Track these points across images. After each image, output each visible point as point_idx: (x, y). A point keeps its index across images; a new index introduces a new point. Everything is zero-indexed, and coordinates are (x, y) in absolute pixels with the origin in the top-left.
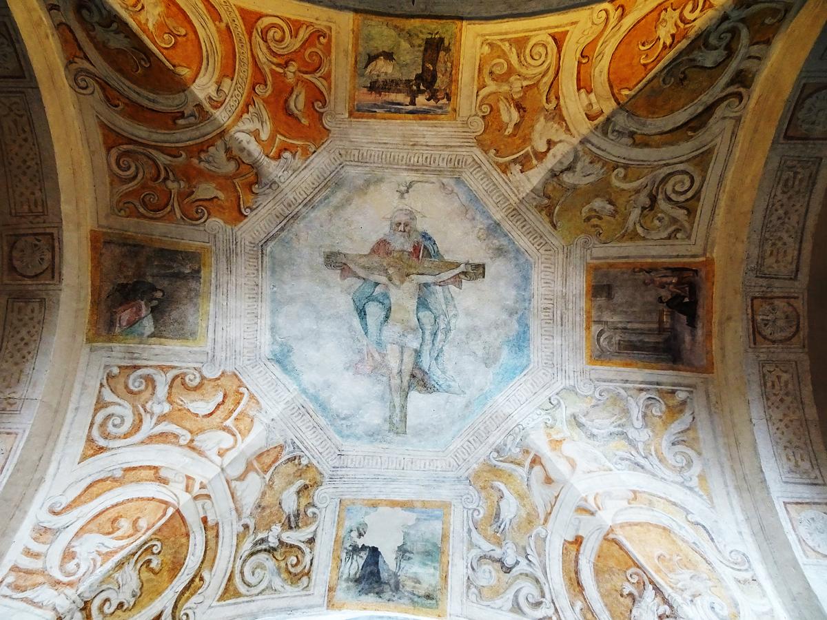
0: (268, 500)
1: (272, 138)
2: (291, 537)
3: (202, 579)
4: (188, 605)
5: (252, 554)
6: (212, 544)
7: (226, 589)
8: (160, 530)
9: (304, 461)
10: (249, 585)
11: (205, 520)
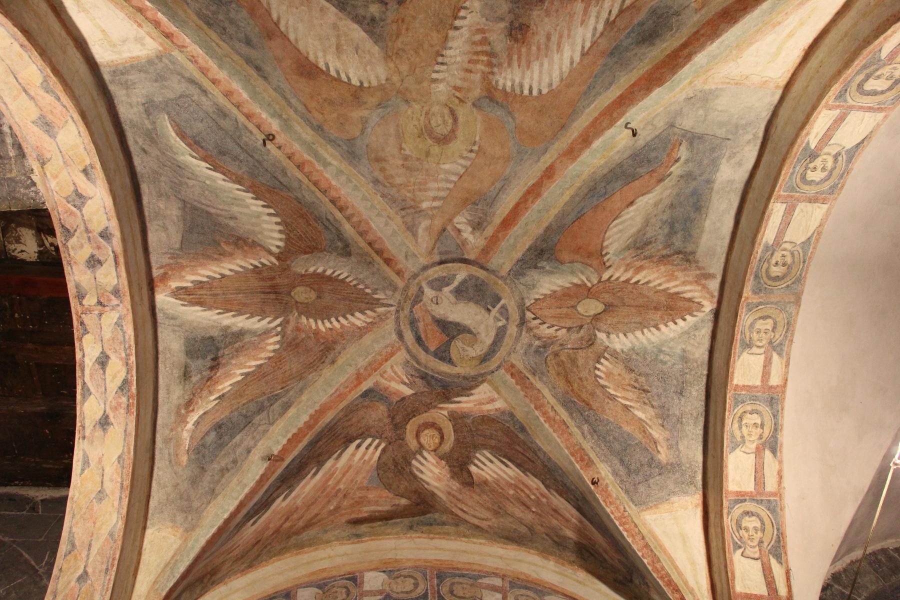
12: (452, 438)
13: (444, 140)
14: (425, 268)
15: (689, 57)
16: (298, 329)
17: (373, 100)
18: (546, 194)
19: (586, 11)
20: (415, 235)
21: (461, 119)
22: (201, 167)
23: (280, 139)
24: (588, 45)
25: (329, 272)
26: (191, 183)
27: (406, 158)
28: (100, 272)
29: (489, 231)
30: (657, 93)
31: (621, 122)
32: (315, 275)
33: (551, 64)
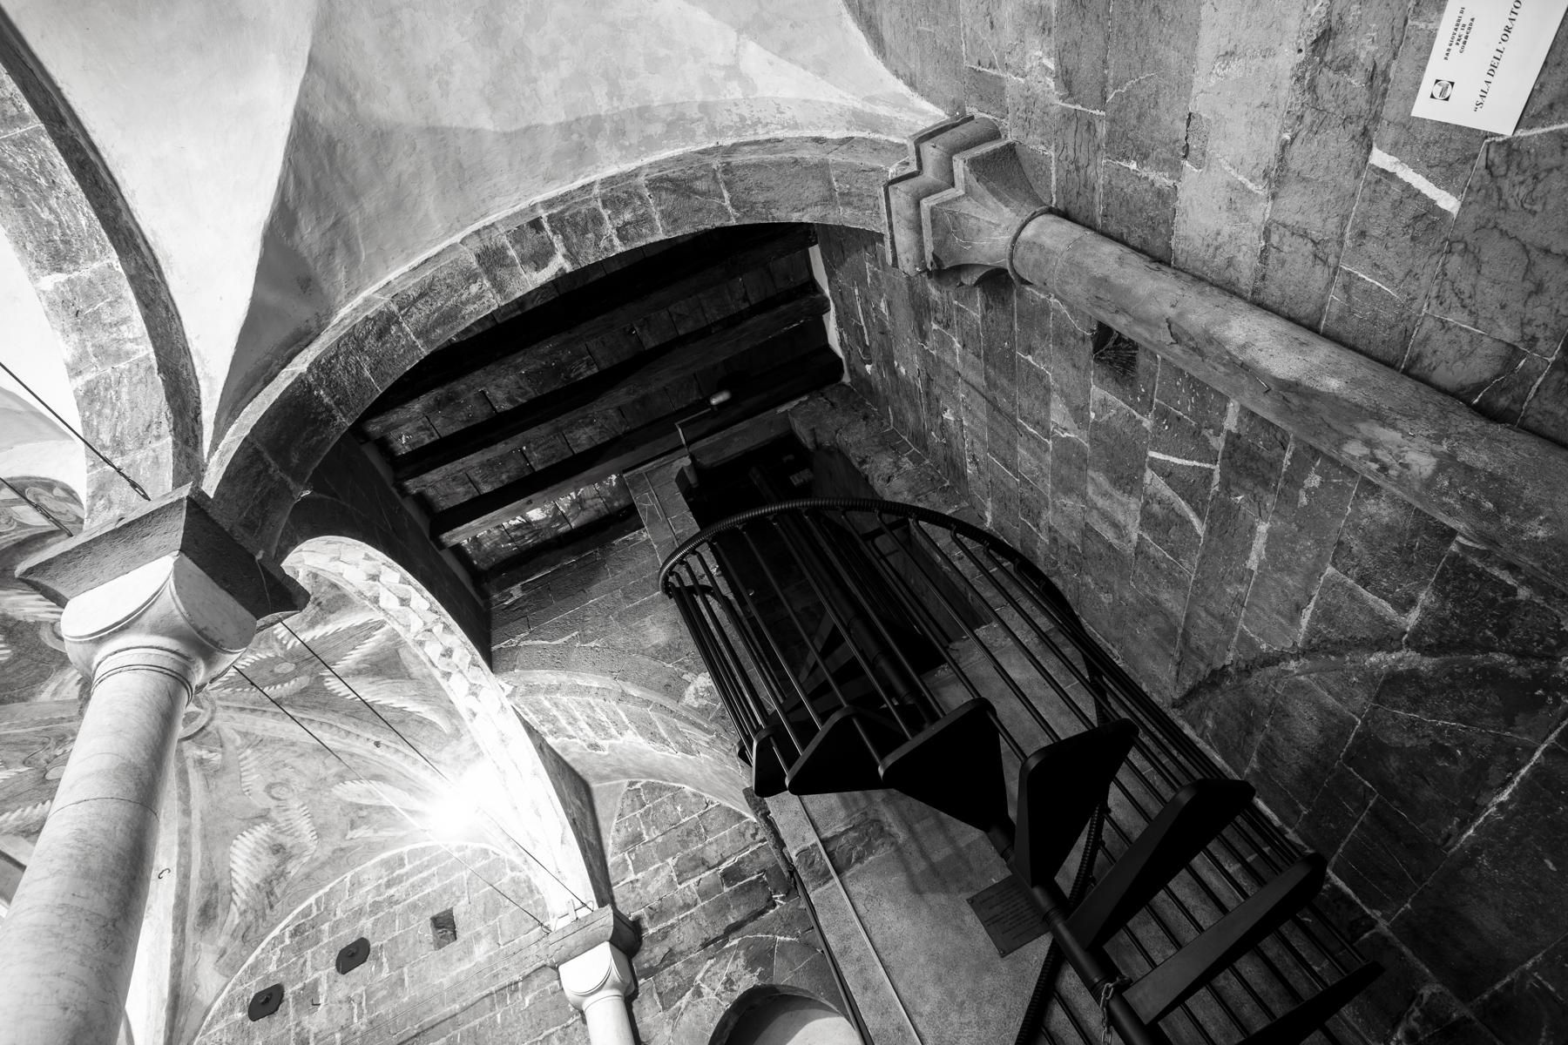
12: (50, 644)
13: (269, 787)
14: (211, 719)
15: (175, 931)
16: (270, 648)
17: (330, 780)
18: (176, 802)
19: (251, 883)
20: (239, 733)
21: (270, 799)
22: (412, 707)
23: (371, 744)
24: (233, 874)
25: (279, 687)
26: (413, 693)
27: (285, 765)
28: (440, 649)
29: (190, 763)
30: (172, 901)
31: (175, 870)
32: (288, 681)
33: (246, 854)
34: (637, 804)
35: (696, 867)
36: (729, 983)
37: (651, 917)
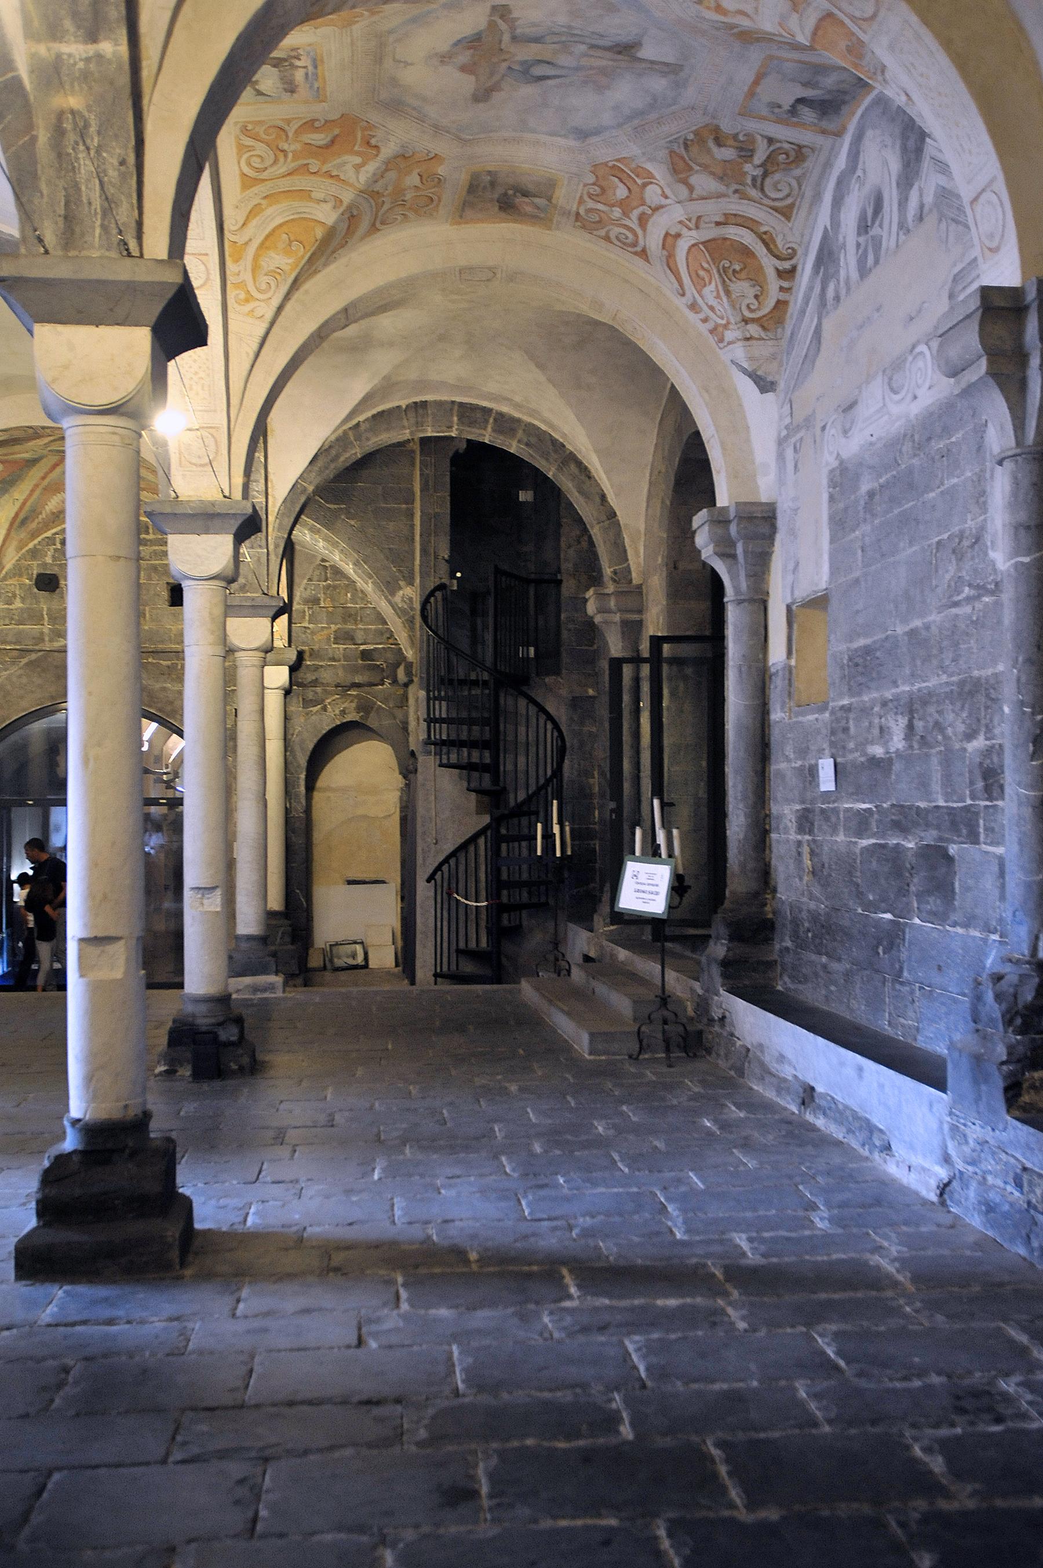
0: (719, 171)
1: (358, 154)
2: (759, 157)
3: (765, 233)
4: (780, 246)
5: (762, 190)
6: (740, 221)
7: (784, 214)
8: (713, 259)
9: (691, 136)
10: (788, 196)
11: (718, 224)
30: (12, 514)
34: (323, 578)
35: (346, 639)
36: (343, 712)
37: (311, 655)
